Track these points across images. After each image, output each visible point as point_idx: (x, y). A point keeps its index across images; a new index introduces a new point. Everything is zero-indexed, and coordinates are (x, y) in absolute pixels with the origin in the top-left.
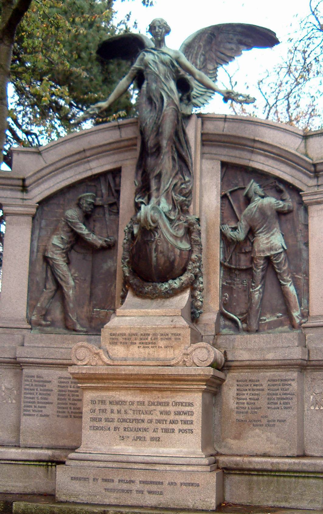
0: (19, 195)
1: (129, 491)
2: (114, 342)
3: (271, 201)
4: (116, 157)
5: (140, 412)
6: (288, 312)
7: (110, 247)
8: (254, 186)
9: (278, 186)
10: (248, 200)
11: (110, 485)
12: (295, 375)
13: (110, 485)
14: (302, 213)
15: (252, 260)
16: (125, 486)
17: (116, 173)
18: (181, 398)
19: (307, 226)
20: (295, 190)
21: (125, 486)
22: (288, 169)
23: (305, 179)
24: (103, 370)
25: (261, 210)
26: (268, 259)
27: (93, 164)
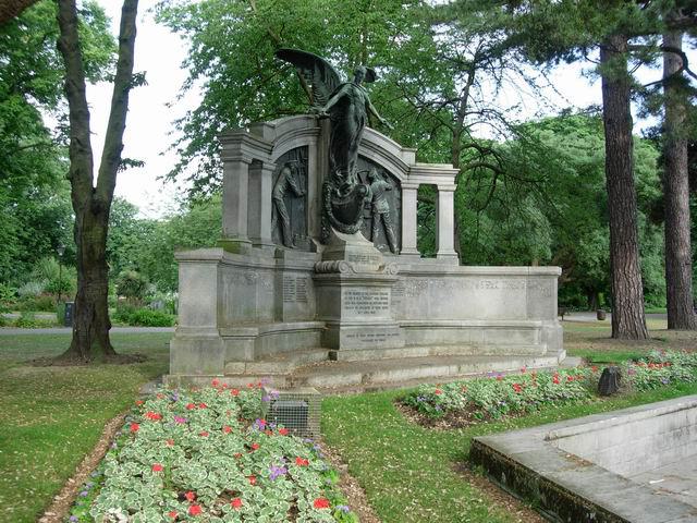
0: (267, 155)
1: (371, 341)
2: (351, 260)
3: (383, 182)
4: (304, 139)
5: (365, 298)
6: (389, 243)
7: (305, 196)
8: (375, 172)
9: (386, 174)
10: (371, 180)
11: (364, 338)
12: (405, 278)
13: (364, 338)
14: (396, 193)
15: (372, 214)
16: (370, 338)
17: (306, 148)
18: (383, 290)
19: (401, 200)
20: (398, 182)
21: (370, 338)
22: (393, 167)
23: (402, 174)
24: (356, 276)
25: (380, 187)
26: (382, 215)
27: (297, 141)
